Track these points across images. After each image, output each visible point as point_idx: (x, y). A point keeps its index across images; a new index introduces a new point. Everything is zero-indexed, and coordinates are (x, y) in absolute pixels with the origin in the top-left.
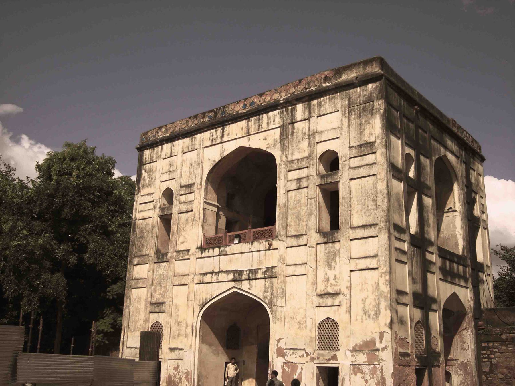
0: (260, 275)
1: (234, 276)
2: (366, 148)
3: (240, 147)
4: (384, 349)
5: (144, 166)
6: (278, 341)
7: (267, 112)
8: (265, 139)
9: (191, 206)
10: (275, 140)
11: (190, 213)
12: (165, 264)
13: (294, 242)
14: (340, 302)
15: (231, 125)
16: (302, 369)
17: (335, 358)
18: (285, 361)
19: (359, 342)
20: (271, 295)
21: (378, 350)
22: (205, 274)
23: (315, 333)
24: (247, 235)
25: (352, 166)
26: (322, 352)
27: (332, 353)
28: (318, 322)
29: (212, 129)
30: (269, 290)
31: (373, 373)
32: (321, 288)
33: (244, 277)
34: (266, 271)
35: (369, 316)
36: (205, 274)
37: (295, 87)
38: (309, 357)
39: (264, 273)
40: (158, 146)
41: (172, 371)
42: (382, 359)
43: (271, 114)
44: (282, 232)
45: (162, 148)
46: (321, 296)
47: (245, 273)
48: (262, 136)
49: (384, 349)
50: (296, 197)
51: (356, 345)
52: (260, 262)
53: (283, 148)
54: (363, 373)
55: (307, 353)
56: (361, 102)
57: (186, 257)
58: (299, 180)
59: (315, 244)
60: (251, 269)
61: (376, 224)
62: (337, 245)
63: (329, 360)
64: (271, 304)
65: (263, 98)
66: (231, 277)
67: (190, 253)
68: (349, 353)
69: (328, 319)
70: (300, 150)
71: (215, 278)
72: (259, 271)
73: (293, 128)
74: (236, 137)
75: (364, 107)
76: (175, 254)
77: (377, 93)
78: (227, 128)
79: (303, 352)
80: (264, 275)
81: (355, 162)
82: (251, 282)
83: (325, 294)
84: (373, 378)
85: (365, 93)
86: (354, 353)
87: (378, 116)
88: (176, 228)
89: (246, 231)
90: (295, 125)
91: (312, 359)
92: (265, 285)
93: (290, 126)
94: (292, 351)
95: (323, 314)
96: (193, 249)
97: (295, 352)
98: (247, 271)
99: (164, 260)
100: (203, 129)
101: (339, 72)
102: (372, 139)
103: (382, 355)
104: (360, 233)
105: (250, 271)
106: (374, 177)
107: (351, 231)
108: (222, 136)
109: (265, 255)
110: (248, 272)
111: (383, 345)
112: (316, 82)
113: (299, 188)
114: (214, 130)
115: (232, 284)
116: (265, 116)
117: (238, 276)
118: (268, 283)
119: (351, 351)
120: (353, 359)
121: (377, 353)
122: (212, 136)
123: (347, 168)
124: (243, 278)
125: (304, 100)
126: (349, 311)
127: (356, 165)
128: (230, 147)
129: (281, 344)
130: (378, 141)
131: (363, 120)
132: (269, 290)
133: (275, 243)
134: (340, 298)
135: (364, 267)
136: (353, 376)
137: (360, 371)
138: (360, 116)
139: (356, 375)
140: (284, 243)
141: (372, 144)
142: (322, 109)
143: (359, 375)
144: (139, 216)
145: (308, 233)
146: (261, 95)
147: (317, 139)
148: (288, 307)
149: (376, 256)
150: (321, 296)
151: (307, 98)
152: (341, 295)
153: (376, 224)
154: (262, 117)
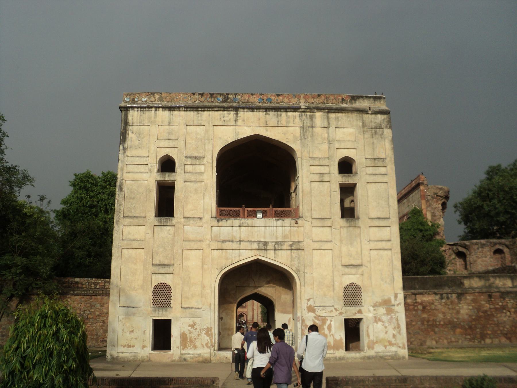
0: (285, 247)
1: (259, 246)
2: (377, 161)
3: (257, 135)
4: (398, 305)
5: (131, 127)
6: (309, 300)
7: (286, 111)
8: (285, 134)
9: (201, 177)
10: (294, 137)
11: (199, 184)
12: (168, 228)
14: (363, 271)
15: (245, 113)
16: (331, 321)
17: (360, 312)
18: (315, 316)
19: (379, 300)
20: (299, 263)
21: (394, 305)
22: (224, 241)
24: (268, 212)
25: (368, 173)
26: (349, 308)
27: (358, 308)
28: (345, 285)
29: (224, 111)
30: (296, 260)
31: (390, 321)
32: (346, 261)
33: (270, 246)
34: (293, 244)
35: (386, 282)
36: (224, 241)
37: (314, 98)
38: (338, 312)
39: (291, 245)
40: (151, 110)
41: (186, 329)
42: (397, 312)
43: (290, 114)
44: (307, 214)
45: (156, 114)
46: (347, 266)
47: (270, 244)
48: (281, 129)
49: (398, 305)
51: (377, 302)
52: (285, 236)
53: (303, 145)
54: (383, 322)
55: (336, 309)
56: (373, 127)
57: (201, 224)
58: (322, 174)
59: (339, 227)
60: (276, 241)
61: (389, 218)
62: (357, 231)
63: (356, 313)
64: (298, 271)
65: (281, 98)
66: (255, 246)
67: (204, 220)
68: (372, 309)
69: (352, 284)
70: (321, 149)
71: (235, 245)
72: (285, 243)
73: (312, 132)
74: (249, 125)
75: (376, 132)
76: (183, 220)
77: (386, 123)
78: (241, 114)
79: (332, 308)
80: (291, 247)
81: (370, 170)
82: (277, 252)
83: (349, 265)
84: (390, 325)
85: (376, 121)
86: (376, 308)
87: (387, 141)
88: (183, 196)
89: (268, 209)
90: (314, 129)
91: (341, 314)
92: (292, 255)
93: (310, 129)
94: (322, 308)
95: (348, 280)
96: (207, 217)
97: (324, 308)
98: (272, 242)
99: (168, 224)
100: (213, 108)
101: (354, 98)
102: (383, 156)
103: (396, 308)
104: (377, 223)
105: (276, 242)
106: (385, 184)
107: (369, 221)
108: (236, 121)
109: (290, 230)
110: (274, 244)
111: (397, 302)
112: (334, 100)
113: (322, 181)
114: (226, 112)
115: (257, 252)
116: (284, 114)
117: (264, 246)
118: (295, 253)
119: (373, 307)
120: (375, 312)
121: (393, 308)
122: (224, 117)
123: (364, 173)
124: (268, 248)
125: (324, 111)
126: (370, 278)
127: (371, 172)
128: (245, 132)
129: (311, 303)
130: (388, 159)
131: (375, 141)
132: (296, 260)
134: (363, 268)
135: (381, 247)
136: (375, 324)
137: (380, 320)
138: (373, 137)
139: (377, 323)
140: (310, 223)
141: (384, 159)
142: (340, 123)
143: (380, 323)
144: (130, 176)
145: (332, 217)
146: (278, 95)
147: (337, 145)
148: (315, 275)
149: (389, 241)
150: (347, 266)
151: (326, 111)
152: (364, 267)
153: (389, 218)
154: (281, 115)
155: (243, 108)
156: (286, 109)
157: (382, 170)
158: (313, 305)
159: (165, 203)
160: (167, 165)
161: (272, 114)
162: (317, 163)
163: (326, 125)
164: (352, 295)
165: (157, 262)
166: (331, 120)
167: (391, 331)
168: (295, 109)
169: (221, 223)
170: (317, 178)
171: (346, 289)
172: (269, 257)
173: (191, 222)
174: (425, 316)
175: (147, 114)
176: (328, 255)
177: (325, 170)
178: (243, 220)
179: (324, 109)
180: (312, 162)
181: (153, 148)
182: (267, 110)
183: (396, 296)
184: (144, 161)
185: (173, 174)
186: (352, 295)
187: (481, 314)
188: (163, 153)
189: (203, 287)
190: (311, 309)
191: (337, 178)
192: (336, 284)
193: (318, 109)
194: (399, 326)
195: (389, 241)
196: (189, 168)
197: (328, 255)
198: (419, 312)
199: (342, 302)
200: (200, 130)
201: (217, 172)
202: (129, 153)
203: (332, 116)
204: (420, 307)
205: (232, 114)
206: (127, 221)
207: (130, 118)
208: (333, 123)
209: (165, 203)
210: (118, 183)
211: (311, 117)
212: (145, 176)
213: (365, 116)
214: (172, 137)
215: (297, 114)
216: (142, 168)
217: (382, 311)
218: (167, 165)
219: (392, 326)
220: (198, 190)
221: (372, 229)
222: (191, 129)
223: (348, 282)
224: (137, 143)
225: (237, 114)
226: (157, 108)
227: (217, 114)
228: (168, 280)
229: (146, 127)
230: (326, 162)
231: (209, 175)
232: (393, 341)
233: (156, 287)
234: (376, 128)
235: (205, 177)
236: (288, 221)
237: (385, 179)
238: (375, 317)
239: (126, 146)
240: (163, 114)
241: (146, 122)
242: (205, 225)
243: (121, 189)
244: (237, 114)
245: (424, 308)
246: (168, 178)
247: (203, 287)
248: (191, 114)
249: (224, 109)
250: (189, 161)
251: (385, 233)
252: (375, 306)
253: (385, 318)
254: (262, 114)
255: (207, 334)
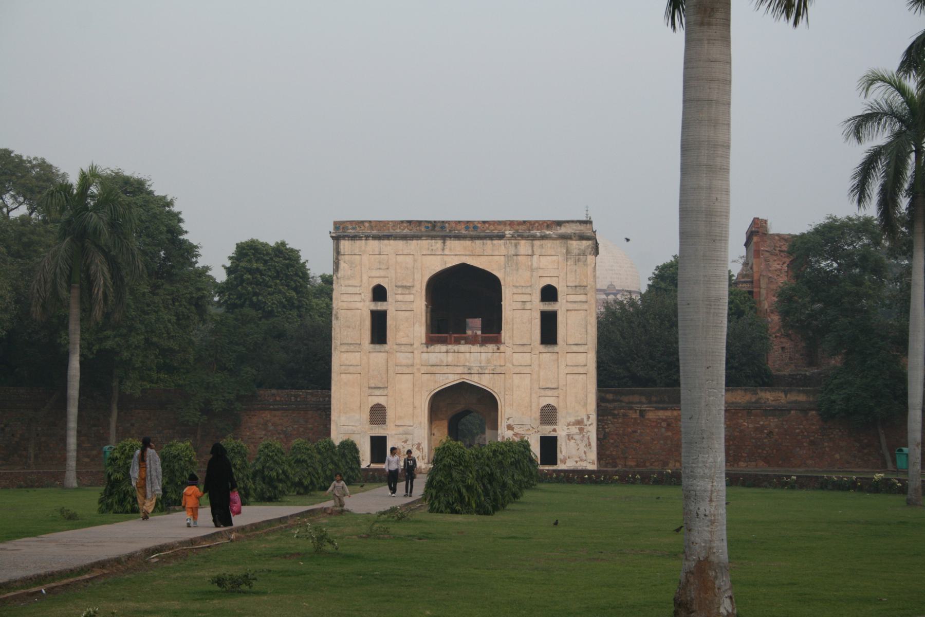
13: (521, 349)
17: (554, 430)
23: (538, 414)
32: (543, 384)
43: (495, 242)
45: (366, 244)
50: (519, 314)
67: (415, 346)
69: (549, 405)
76: (395, 347)
78: (450, 243)
96: (417, 344)
102: (585, 284)
104: (575, 348)
108: (443, 250)
116: (489, 242)
129: (510, 422)
133: (502, 347)
134: (560, 391)
144: (345, 305)
149: (585, 365)
155: (450, 237)
156: (491, 238)
157: (582, 298)
158: (512, 423)
159: (379, 329)
160: (379, 293)
161: (478, 242)
162: (520, 292)
163: (530, 253)
164: (549, 414)
165: (373, 385)
166: (535, 248)
167: (582, 448)
168: (501, 237)
169: (432, 348)
170: (519, 306)
171: (543, 409)
172: (474, 380)
173: (403, 348)
174: (669, 434)
175: (358, 243)
176: (527, 381)
177: (525, 298)
178: (450, 347)
179: (528, 237)
180: (515, 291)
181: (365, 278)
182: (473, 238)
183: (589, 418)
184: (357, 290)
185: (385, 303)
186: (549, 414)
187: (736, 434)
188: (375, 282)
189: (414, 407)
190: (510, 427)
191: (539, 305)
192: (534, 405)
193: (522, 237)
194: (590, 445)
195: (585, 365)
196: (399, 297)
197: (527, 381)
198: (663, 430)
199: (538, 422)
200: (409, 259)
201: (427, 300)
202: (343, 282)
203: (537, 243)
204: (664, 424)
205: (439, 243)
206: (344, 348)
207: (341, 247)
208: (537, 251)
209: (379, 329)
210: (334, 312)
211: (516, 246)
212: (359, 305)
213: (570, 242)
214: (383, 267)
215: (502, 242)
216: (357, 298)
217: (574, 430)
218: (379, 293)
219: (584, 444)
220: (410, 315)
221: (569, 355)
222: (400, 258)
223: (545, 404)
224: (349, 272)
225: (444, 243)
226: (367, 237)
227: (424, 243)
228: (382, 401)
229: (357, 257)
230: (528, 291)
231: (419, 303)
232: (584, 458)
233: (372, 408)
234: (579, 255)
235: (414, 306)
236: (491, 347)
237: (585, 306)
238: (568, 435)
239: (339, 275)
240: (373, 244)
241: (357, 252)
242: (416, 352)
243: (337, 318)
244: (444, 243)
245: (669, 425)
246: (380, 306)
247: (414, 407)
248: (400, 244)
249: (433, 237)
250: (400, 291)
251: (581, 359)
252: (569, 425)
253: (577, 437)
254: (468, 243)
255: (418, 448)
